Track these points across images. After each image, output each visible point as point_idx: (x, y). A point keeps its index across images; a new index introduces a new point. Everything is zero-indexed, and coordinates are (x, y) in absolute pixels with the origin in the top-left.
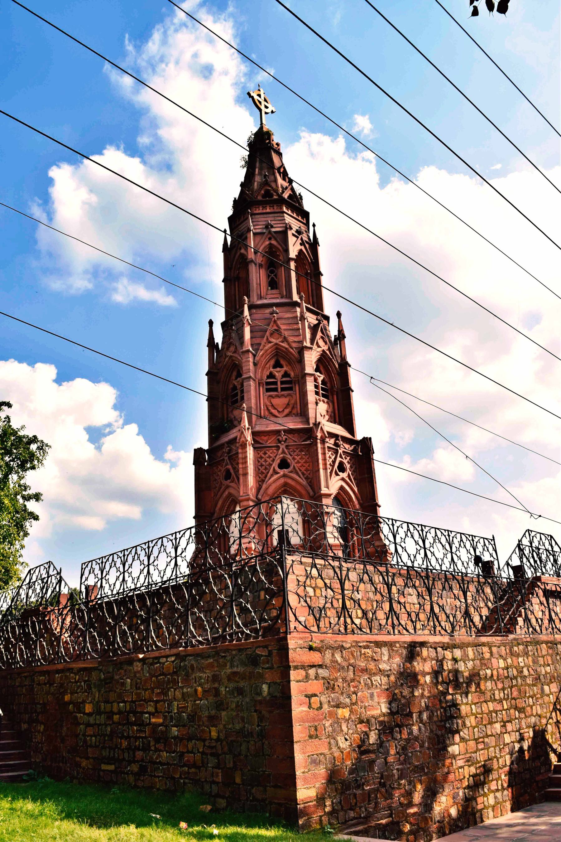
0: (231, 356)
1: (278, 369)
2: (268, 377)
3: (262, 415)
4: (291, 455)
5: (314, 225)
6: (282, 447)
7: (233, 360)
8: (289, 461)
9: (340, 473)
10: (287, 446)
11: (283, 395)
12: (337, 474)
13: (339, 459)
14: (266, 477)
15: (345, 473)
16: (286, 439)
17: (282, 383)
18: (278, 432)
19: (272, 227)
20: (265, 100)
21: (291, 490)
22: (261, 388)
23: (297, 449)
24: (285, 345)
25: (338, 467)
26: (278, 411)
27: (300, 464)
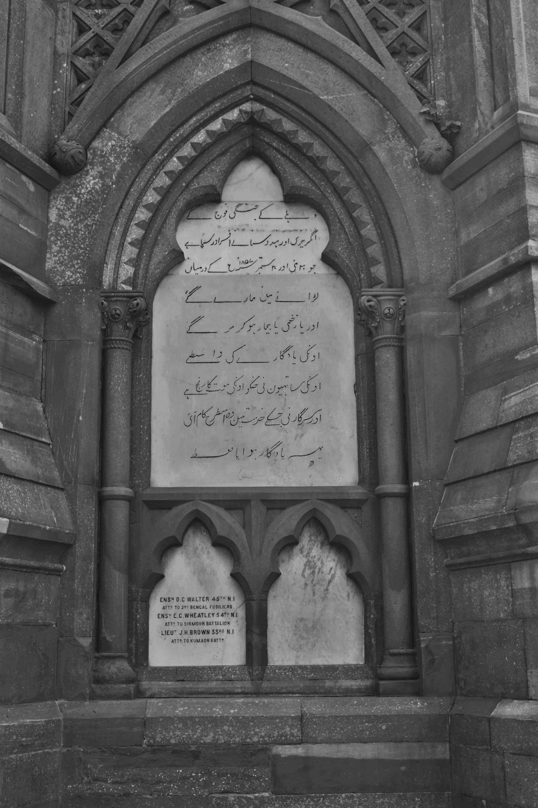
14: (127, 17)
21: (288, 126)
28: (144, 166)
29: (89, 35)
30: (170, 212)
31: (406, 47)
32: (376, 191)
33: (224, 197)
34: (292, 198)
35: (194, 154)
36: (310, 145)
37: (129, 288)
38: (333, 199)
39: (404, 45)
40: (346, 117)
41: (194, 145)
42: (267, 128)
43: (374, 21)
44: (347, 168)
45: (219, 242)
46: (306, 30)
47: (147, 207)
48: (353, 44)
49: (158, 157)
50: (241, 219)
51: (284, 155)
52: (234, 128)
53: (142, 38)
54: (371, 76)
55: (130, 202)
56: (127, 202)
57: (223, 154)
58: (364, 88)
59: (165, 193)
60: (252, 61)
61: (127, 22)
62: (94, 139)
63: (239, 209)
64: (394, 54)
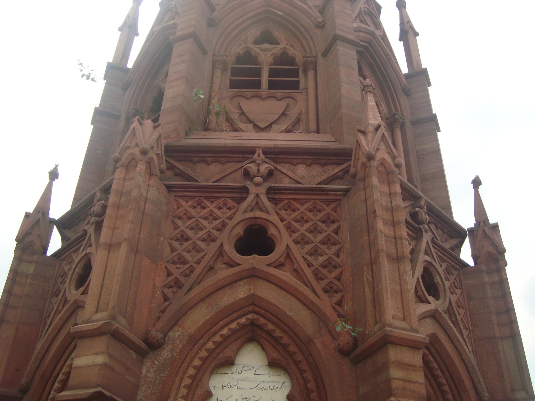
1: (266, 45)
6: (257, 191)
8: (272, 231)
9: (430, 298)
10: (270, 191)
12: (421, 300)
13: (422, 258)
14: (192, 270)
15: (440, 302)
16: (270, 173)
17: (272, 73)
18: (246, 153)
21: (270, 327)
22: (218, 73)
23: (302, 202)
27: (308, 247)
28: (194, 346)
29: (172, 278)
30: (206, 370)
31: (332, 288)
32: (316, 364)
33: (236, 363)
34: (273, 364)
35: (221, 340)
36: (281, 338)
38: (293, 366)
39: (331, 287)
40: (301, 325)
41: (221, 336)
42: (260, 327)
43: (316, 275)
44: (301, 351)
45: (232, 386)
46: (281, 279)
47: (195, 367)
48: (305, 287)
49: (202, 341)
50: (245, 374)
51: (268, 341)
52: (243, 327)
53: (198, 281)
54: (312, 303)
55: (185, 365)
56: (184, 365)
57: (236, 340)
58: (310, 309)
59: (204, 360)
60: (253, 294)
61: (192, 272)
62: (169, 331)
63: (244, 369)
64: (326, 292)
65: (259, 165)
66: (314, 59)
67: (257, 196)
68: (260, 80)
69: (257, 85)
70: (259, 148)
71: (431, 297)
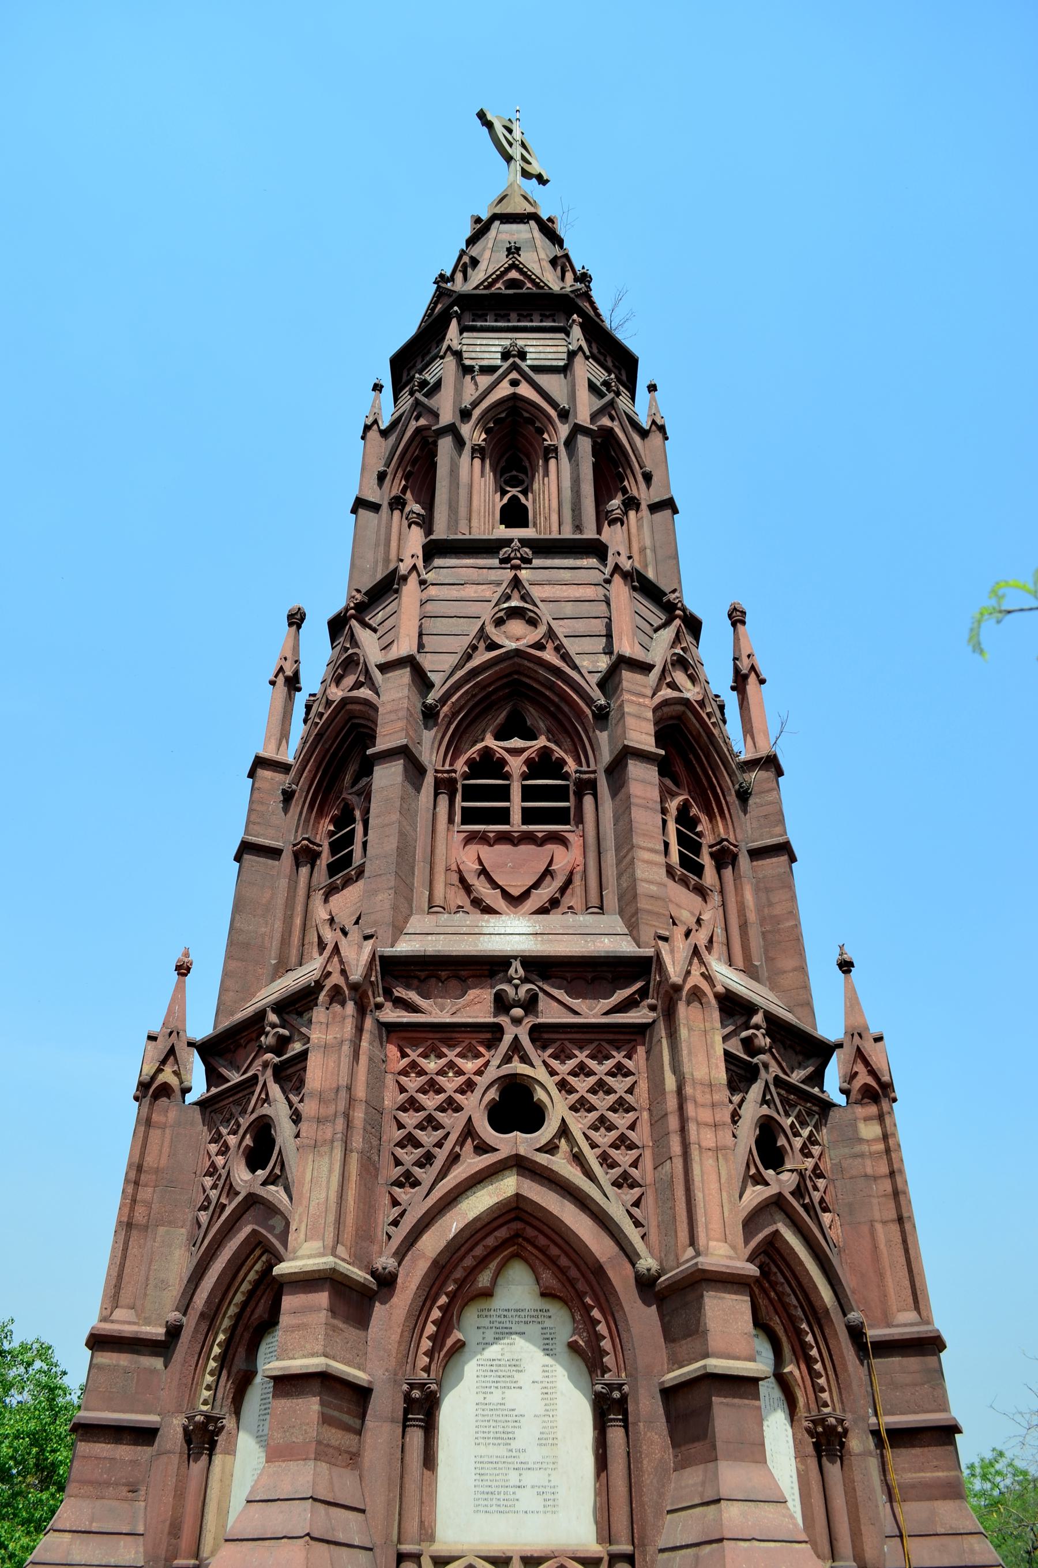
0: (344, 701)
1: (516, 743)
2: (476, 768)
3: (438, 900)
4: (553, 1073)
5: (652, 388)
6: (516, 1031)
7: (352, 716)
8: (540, 1094)
11: (528, 838)
17: (528, 793)
19: (522, 355)
20: (523, 145)
22: (443, 801)
24: (549, 655)
25: (757, 1142)
26: (506, 895)
37: (425, 1375)
65: (517, 987)
66: (592, 776)
67: (516, 1037)
68: (508, 809)
69: (503, 816)
70: (515, 957)
71: (771, 1172)
